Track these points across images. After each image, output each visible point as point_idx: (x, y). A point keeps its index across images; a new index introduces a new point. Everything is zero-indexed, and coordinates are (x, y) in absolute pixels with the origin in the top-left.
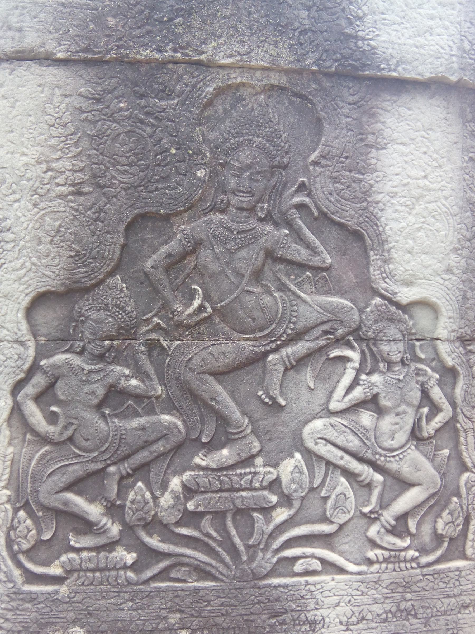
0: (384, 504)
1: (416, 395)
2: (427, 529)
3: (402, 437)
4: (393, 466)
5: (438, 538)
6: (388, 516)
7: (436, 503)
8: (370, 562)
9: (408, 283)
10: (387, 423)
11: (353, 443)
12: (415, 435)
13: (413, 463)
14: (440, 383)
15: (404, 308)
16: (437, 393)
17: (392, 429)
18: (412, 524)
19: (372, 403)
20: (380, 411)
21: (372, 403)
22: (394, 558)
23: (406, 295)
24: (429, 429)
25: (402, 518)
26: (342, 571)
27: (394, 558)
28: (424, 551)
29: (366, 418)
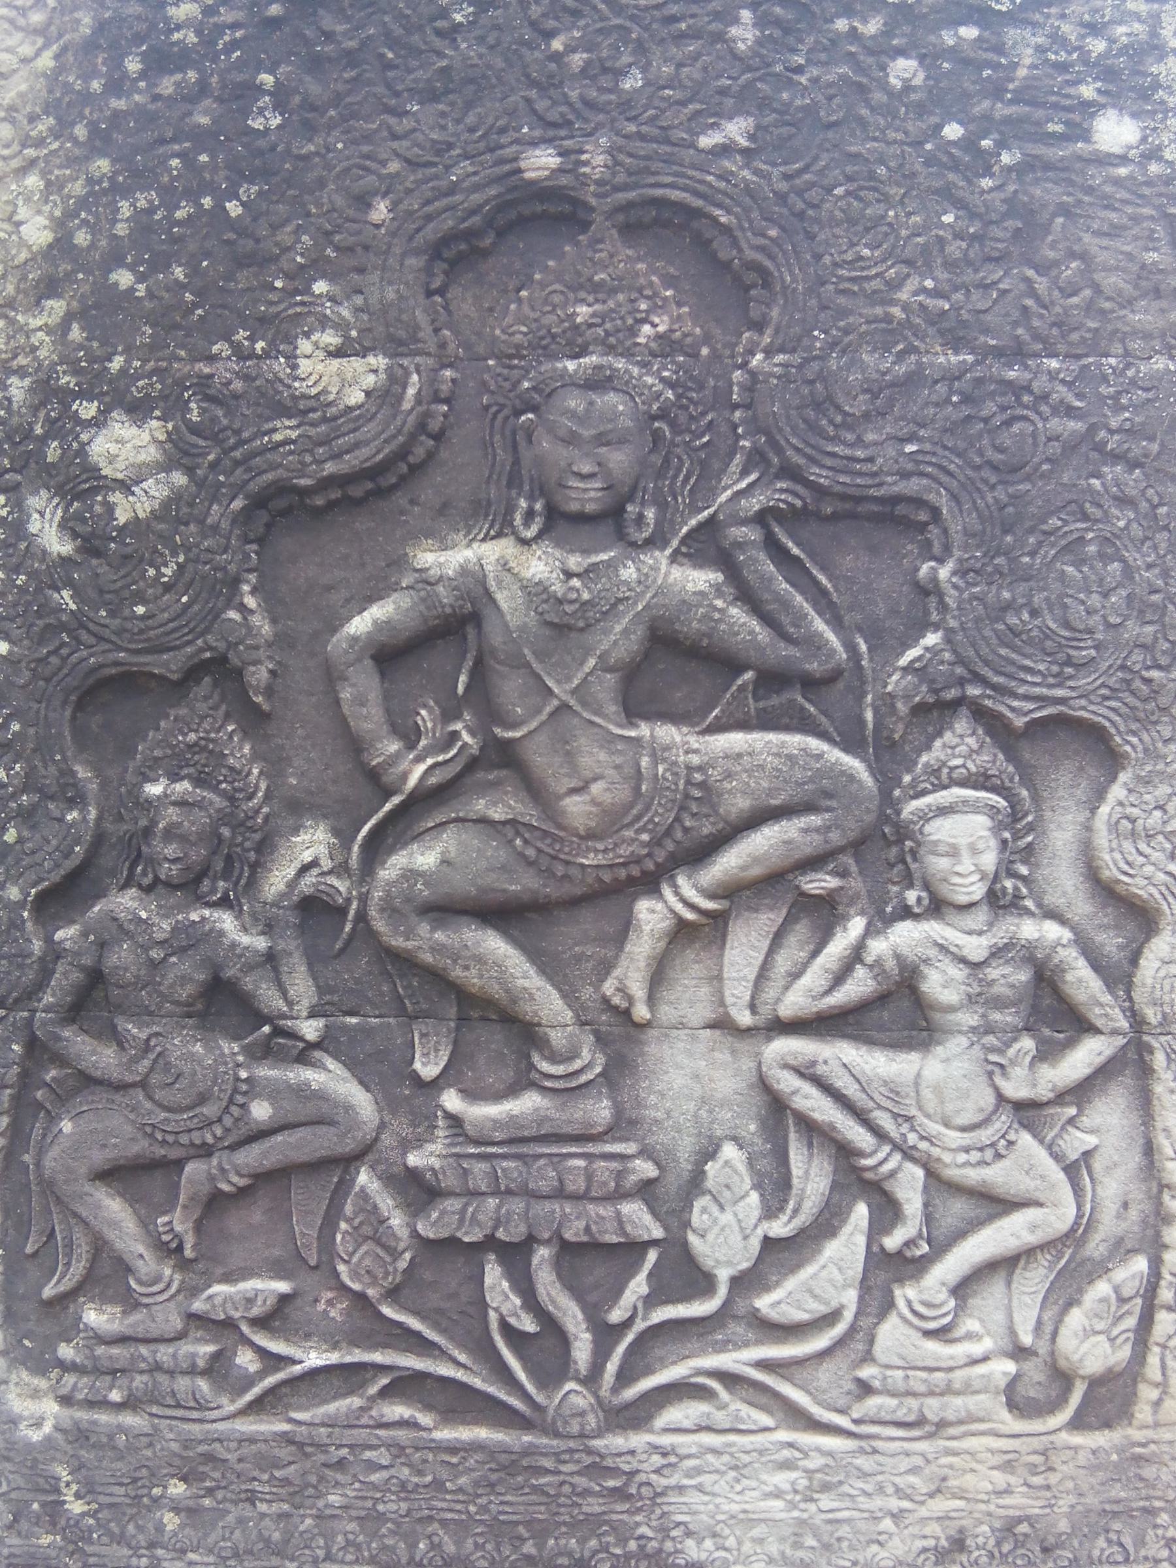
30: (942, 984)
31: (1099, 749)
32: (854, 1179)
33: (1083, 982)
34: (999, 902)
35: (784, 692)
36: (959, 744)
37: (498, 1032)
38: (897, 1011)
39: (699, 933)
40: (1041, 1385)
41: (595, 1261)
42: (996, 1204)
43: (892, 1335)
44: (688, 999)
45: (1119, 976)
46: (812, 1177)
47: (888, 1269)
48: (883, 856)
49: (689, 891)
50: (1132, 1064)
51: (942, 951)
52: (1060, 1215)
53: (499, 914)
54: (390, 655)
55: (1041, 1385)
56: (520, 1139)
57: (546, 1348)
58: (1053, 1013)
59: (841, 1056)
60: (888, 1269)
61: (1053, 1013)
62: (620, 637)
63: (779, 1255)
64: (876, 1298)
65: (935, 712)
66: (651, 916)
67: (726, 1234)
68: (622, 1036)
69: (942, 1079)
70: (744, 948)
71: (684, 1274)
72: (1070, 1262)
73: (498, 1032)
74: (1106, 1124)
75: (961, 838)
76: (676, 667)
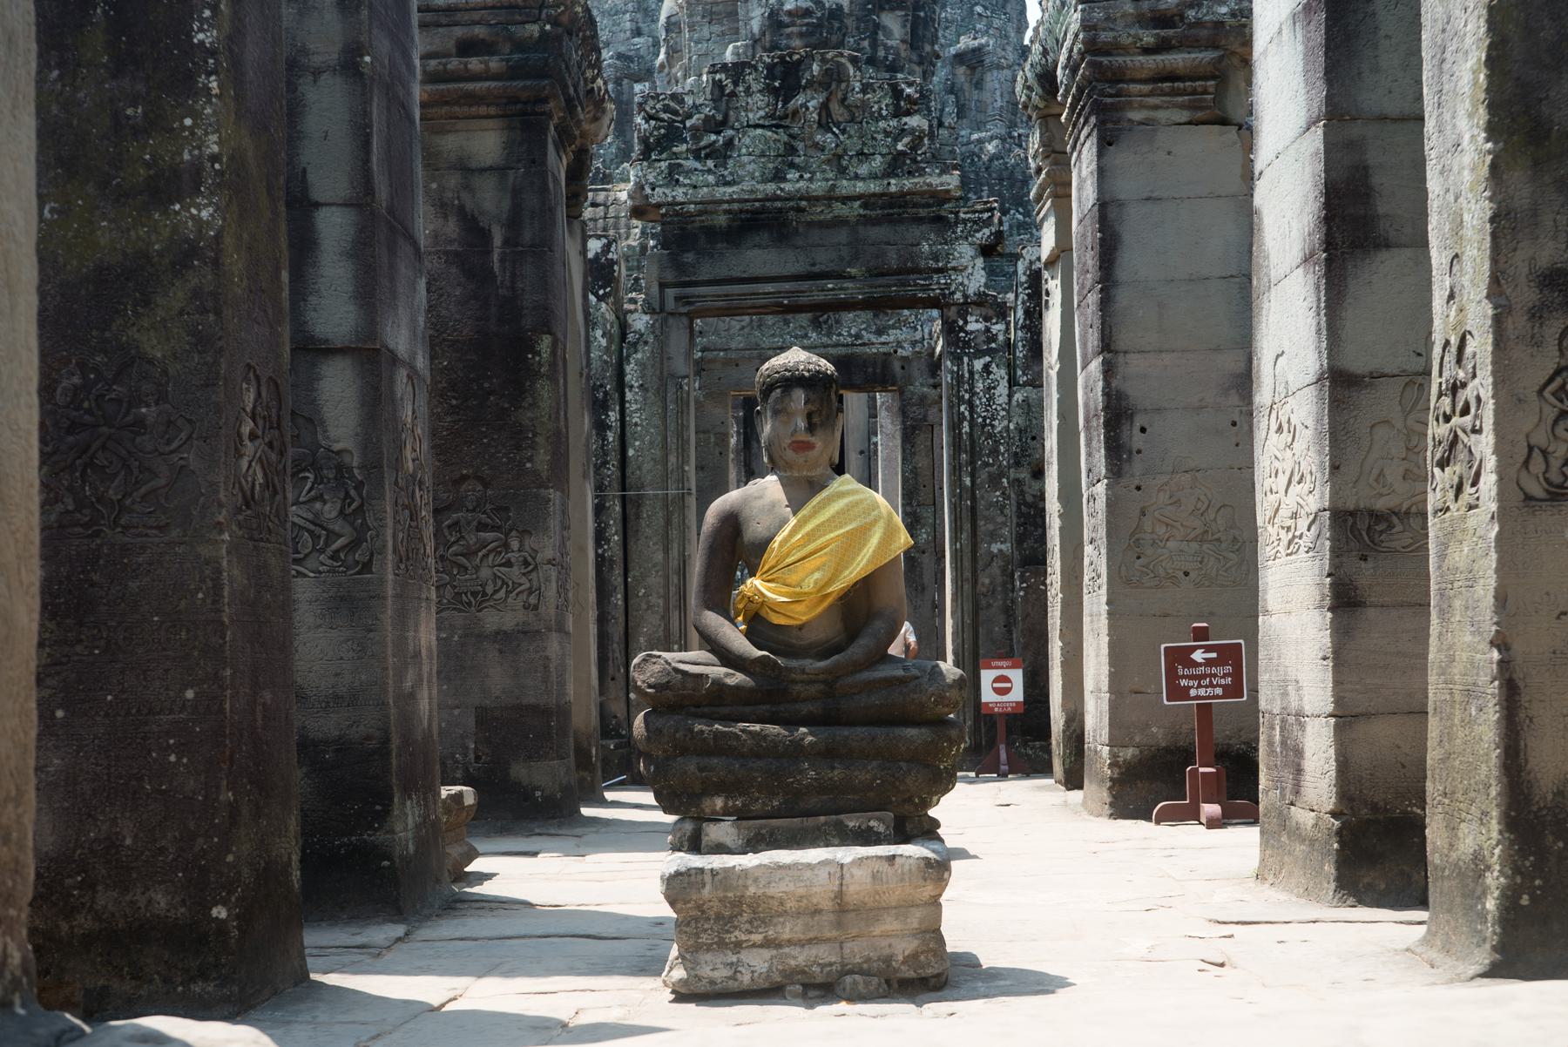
0: (327, 544)
1: (342, 495)
3: (334, 514)
6: (329, 551)
7: (353, 545)
10: (327, 507)
11: (310, 516)
12: (341, 512)
16: (353, 493)
18: (342, 556)
21: (320, 498)
23: (337, 447)
25: (337, 551)
26: (305, 576)
31: (530, 533)
35: (495, 528)
36: (514, 533)
38: (509, 564)
39: (486, 556)
47: (508, 593)
48: (506, 546)
51: (513, 556)
54: (449, 527)
57: (470, 604)
59: (502, 569)
60: (508, 593)
61: (526, 563)
63: (496, 592)
67: (489, 590)
70: (491, 557)
71: (484, 594)
72: (530, 591)
74: (534, 574)
75: (515, 544)
76: (482, 527)
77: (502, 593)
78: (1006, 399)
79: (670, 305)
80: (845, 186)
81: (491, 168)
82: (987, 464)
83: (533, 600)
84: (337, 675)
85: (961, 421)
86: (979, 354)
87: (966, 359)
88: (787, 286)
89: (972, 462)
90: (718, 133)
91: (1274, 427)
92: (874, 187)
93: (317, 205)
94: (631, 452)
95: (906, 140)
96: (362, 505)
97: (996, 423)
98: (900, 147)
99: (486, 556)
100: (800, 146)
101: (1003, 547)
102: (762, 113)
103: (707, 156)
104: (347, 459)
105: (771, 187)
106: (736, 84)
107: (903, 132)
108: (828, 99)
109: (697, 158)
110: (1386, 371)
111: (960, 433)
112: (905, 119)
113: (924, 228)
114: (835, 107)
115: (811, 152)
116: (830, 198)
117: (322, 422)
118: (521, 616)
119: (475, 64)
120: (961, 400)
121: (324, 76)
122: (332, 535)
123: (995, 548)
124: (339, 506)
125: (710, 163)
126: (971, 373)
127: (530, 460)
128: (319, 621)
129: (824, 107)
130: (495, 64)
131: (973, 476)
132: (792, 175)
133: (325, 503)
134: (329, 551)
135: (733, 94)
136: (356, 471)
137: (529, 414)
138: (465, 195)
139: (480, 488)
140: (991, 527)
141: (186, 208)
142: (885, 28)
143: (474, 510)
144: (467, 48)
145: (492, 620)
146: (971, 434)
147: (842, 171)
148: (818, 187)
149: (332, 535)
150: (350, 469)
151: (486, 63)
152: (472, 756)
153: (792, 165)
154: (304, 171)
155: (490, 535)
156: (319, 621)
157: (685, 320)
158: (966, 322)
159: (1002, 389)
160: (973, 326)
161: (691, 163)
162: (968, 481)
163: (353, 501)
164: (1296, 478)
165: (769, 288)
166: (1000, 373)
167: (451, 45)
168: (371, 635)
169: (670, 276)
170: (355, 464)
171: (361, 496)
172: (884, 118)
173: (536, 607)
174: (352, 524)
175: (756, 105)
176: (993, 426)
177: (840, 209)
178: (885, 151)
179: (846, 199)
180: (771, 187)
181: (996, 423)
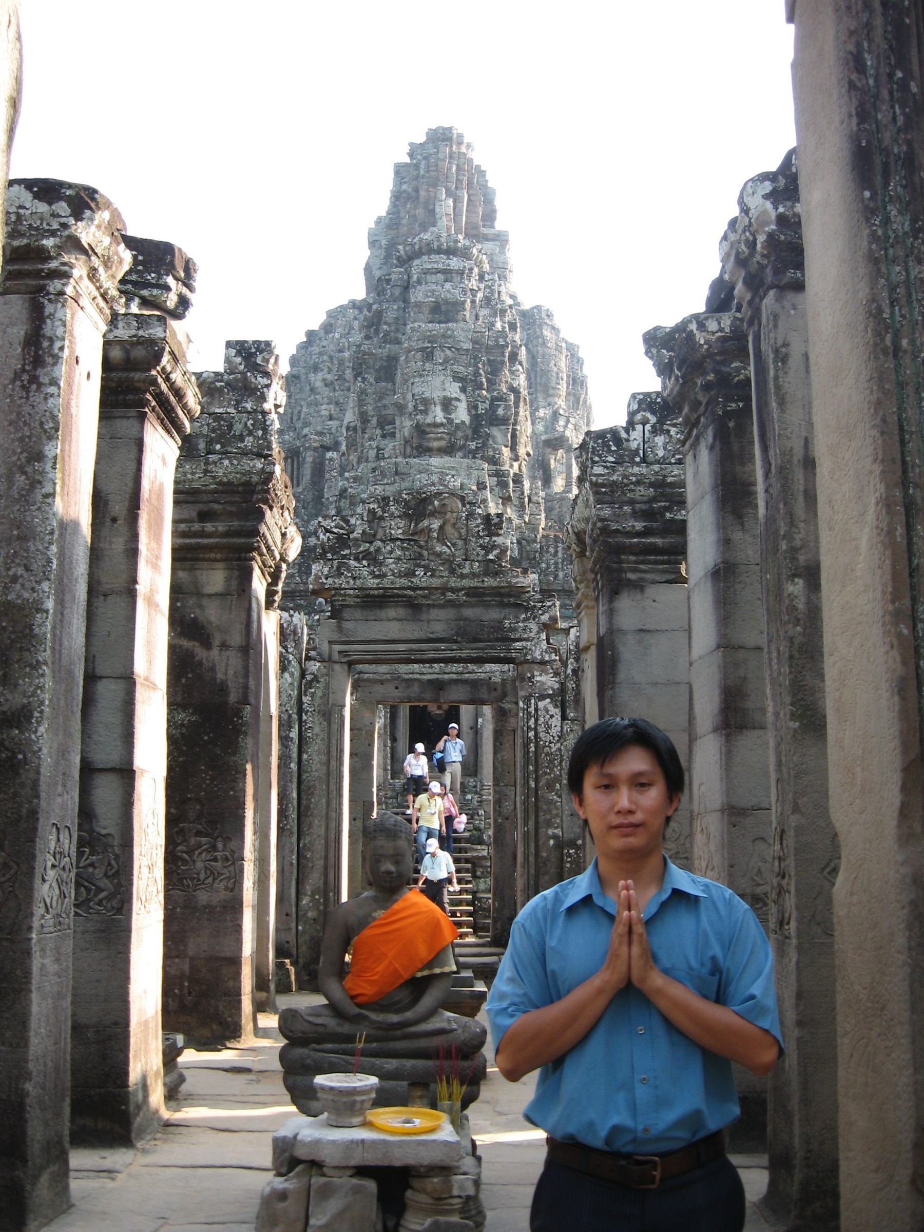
0: (96, 895)
1: (106, 863)
2: (109, 905)
3: (101, 875)
4: (98, 884)
5: (113, 908)
6: (96, 900)
8: (90, 914)
9: (105, 828)
10: (97, 871)
12: (106, 875)
13: (104, 883)
14: (115, 859)
15: (104, 836)
16: (113, 862)
17: (99, 873)
18: (104, 902)
19: (92, 865)
20: (95, 868)
22: (98, 913)
23: (104, 832)
24: (110, 873)
25: (101, 901)
27: (98, 913)
28: (108, 911)
29: (90, 870)
30: (219, 857)
31: (230, 839)
32: (212, 873)
33: (229, 857)
34: (223, 851)
35: (206, 836)
36: (220, 839)
37: (185, 862)
38: (215, 860)
39: (200, 854)
40: (227, 888)
41: (192, 879)
42: (223, 874)
43: (215, 885)
44: (200, 859)
45: (233, 857)
46: (208, 872)
47: (214, 879)
48: (214, 848)
49: (200, 850)
50: (233, 863)
51: (218, 854)
52: (228, 875)
53: (186, 852)
54: (177, 832)
55: (227, 888)
56: (186, 870)
57: (188, 886)
58: (227, 859)
60: (214, 879)
61: (227, 859)
62: (195, 831)
63: (206, 878)
64: (214, 882)
65: (218, 837)
66: (197, 852)
67: (202, 876)
68: (194, 862)
69: (219, 864)
70: (204, 855)
71: (199, 880)
72: (229, 878)
73: (185, 862)
74: (231, 868)
75: (220, 845)
76: (199, 834)
77: (210, 880)
78: (559, 729)
79: (336, 656)
80: (454, 582)
81: (216, 594)
82: (546, 773)
83: (230, 886)
84: (98, 981)
85: (528, 744)
86: (542, 697)
87: (533, 701)
88: (414, 646)
89: (536, 771)
90: (371, 543)
91: (699, 829)
92: (474, 583)
93: (101, 678)
94: (305, 756)
95: (495, 552)
96: (118, 871)
97: (552, 745)
98: (491, 557)
99: (200, 854)
100: (425, 553)
101: (555, 831)
102: (400, 531)
103: (364, 558)
104: (110, 840)
105: (404, 582)
106: (384, 511)
107: (494, 547)
108: (444, 524)
109: (357, 559)
110: (763, 806)
111: (528, 752)
112: (494, 539)
113: (507, 610)
114: (449, 529)
115: (431, 558)
116: (444, 589)
117: (95, 817)
118: (223, 895)
119: (209, 527)
120: (529, 728)
121: (110, 598)
122: (99, 890)
123: (550, 832)
124: (104, 868)
125: (365, 563)
126: (536, 710)
127: (233, 789)
128: (88, 946)
129: (441, 528)
130: (221, 527)
131: (537, 781)
132: (420, 572)
133: (95, 868)
134: (96, 900)
135: (382, 518)
136: (116, 848)
137: (233, 758)
138: (198, 611)
139: (198, 807)
140: (548, 817)
141: (21, 732)
142: (494, 438)
143: (194, 822)
144: (204, 516)
145: (203, 897)
146: (536, 752)
147: (452, 571)
148: (436, 582)
149: (99, 890)
150: (112, 846)
151: (216, 527)
152: (186, 991)
153: (419, 566)
154: (94, 657)
155: (204, 840)
156: (88, 946)
157: (346, 667)
158: (533, 676)
159: (556, 722)
160: (538, 678)
161: (353, 563)
162: (533, 784)
163: (112, 868)
164: (710, 867)
165: (402, 647)
166: (556, 712)
167: (194, 515)
168: (120, 956)
169: (335, 637)
170: (115, 844)
171: (118, 864)
172: (481, 537)
173: (232, 890)
174: (111, 883)
175: (397, 528)
176: (550, 747)
177: (450, 596)
178: (480, 558)
179: (453, 590)
180: (404, 582)
181: (552, 745)
